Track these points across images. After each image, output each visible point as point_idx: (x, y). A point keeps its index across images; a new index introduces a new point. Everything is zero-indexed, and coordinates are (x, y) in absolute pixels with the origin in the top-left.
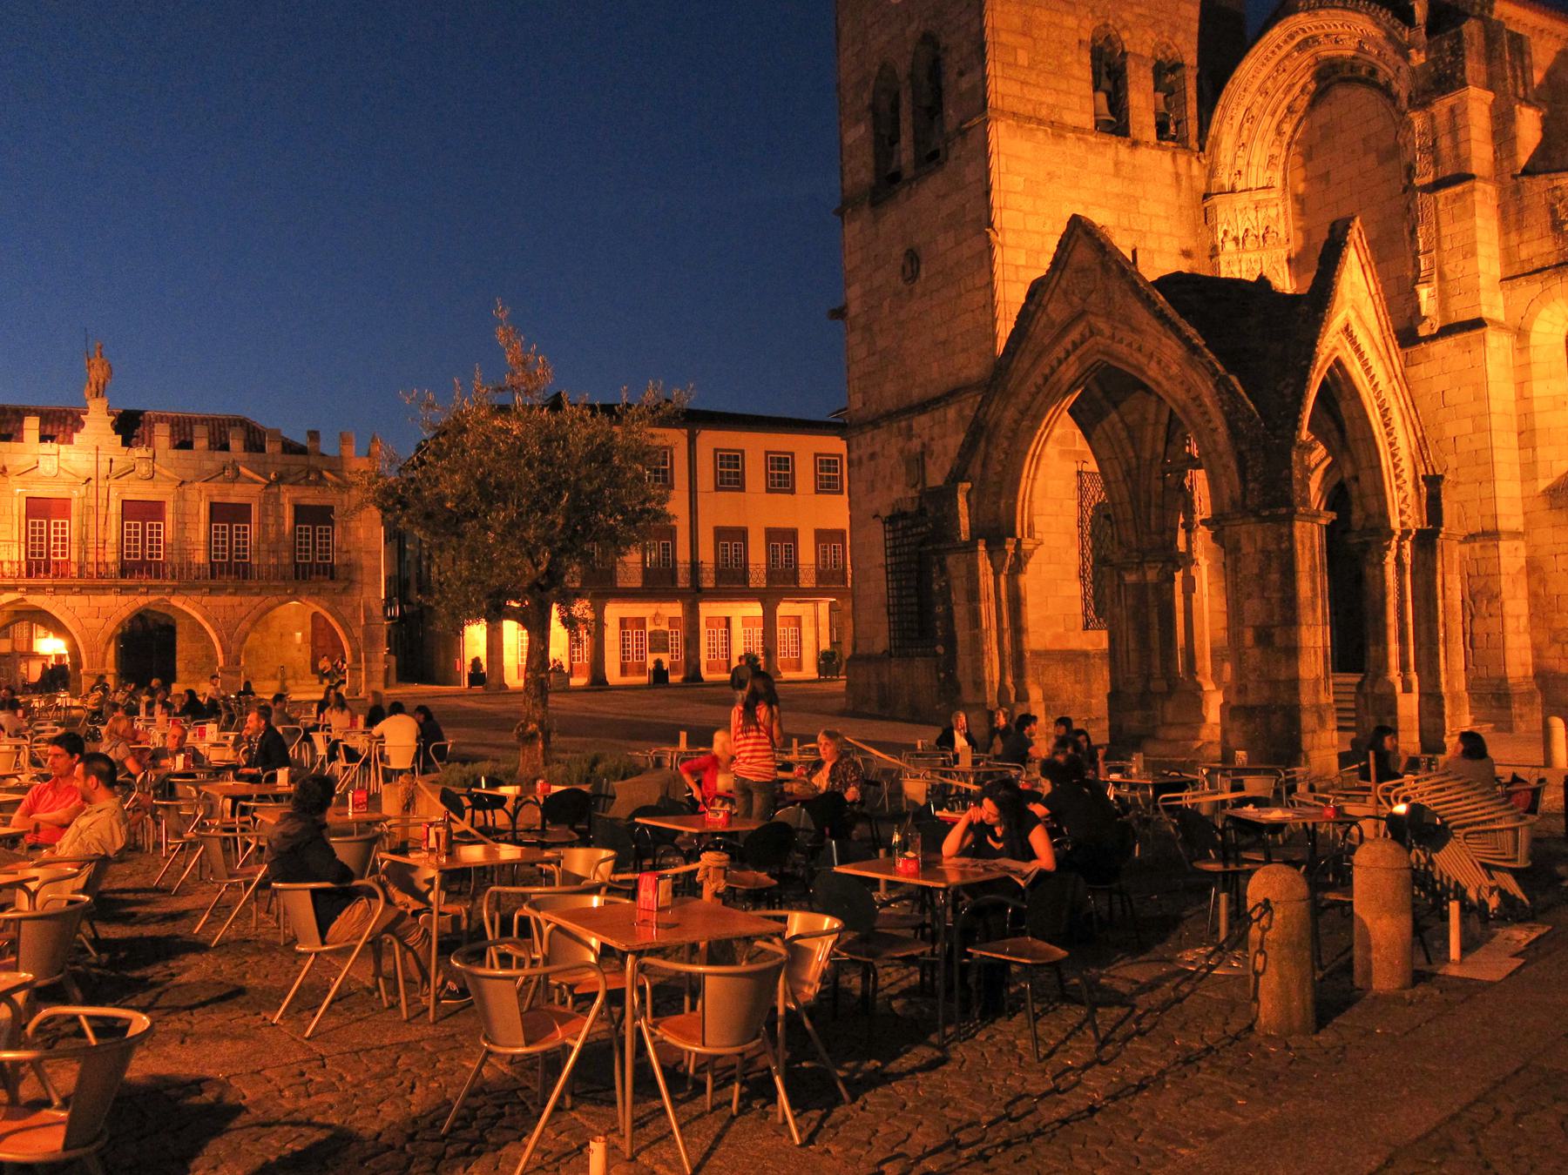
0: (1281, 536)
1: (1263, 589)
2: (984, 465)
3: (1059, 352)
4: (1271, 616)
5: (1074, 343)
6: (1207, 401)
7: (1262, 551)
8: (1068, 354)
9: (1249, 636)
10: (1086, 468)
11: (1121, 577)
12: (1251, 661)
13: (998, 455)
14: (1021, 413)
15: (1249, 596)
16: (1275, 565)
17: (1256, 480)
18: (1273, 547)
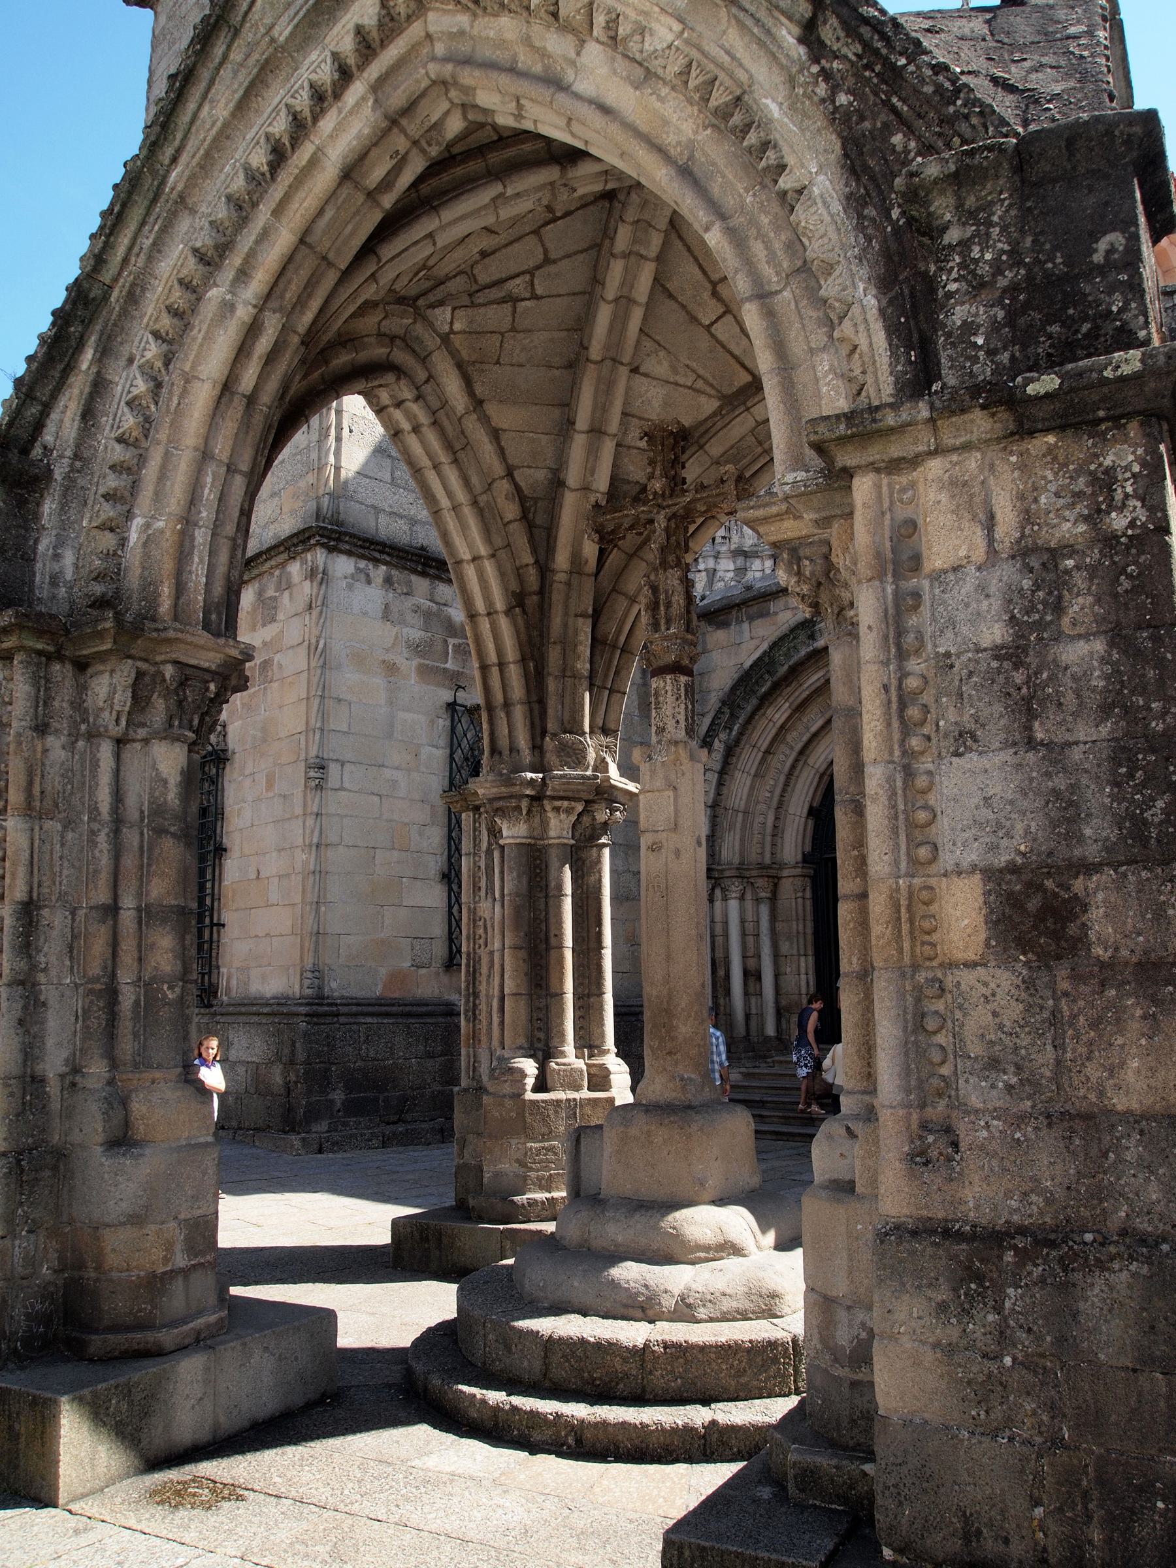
0: (1105, 481)
1: (1027, 708)
2: (88, 414)
3: (316, 66)
4: (1066, 812)
5: (359, 31)
6: (773, 107)
7: (1023, 552)
8: (345, 75)
9: (962, 914)
10: (462, 697)
11: (495, 833)
12: (977, 1020)
13: (128, 382)
14: (201, 257)
15: (965, 740)
16: (1080, 605)
17: (977, 287)
18: (1070, 528)
